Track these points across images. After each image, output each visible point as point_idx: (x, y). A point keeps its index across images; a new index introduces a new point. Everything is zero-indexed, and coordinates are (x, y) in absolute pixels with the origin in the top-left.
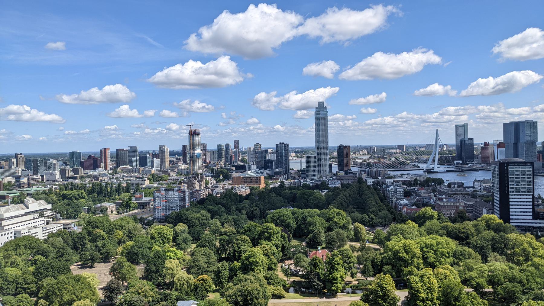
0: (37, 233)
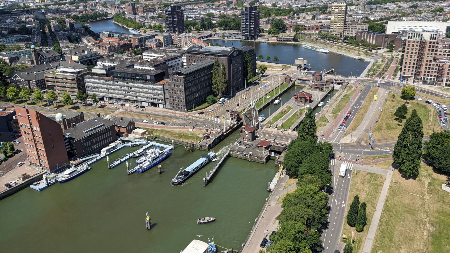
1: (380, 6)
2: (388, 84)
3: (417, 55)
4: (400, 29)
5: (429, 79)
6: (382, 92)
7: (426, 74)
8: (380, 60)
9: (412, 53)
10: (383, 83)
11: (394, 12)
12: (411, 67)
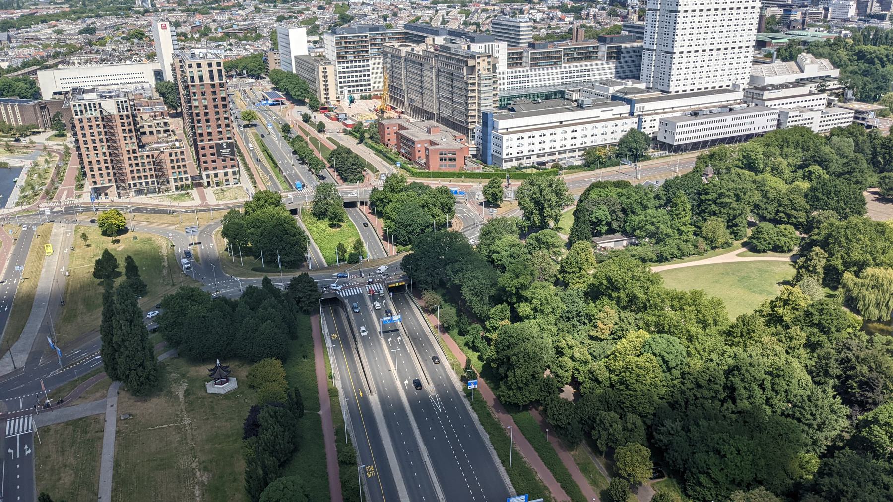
0: (812, 119)
1: (17, 32)
2: (70, 210)
3: (105, 144)
4: (68, 85)
5: (144, 184)
6: (60, 231)
7: (136, 175)
8: (41, 160)
9: (94, 141)
10: (58, 212)
11: (49, 45)
12: (104, 168)
